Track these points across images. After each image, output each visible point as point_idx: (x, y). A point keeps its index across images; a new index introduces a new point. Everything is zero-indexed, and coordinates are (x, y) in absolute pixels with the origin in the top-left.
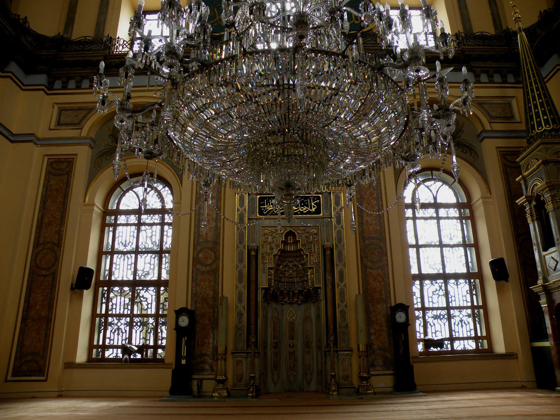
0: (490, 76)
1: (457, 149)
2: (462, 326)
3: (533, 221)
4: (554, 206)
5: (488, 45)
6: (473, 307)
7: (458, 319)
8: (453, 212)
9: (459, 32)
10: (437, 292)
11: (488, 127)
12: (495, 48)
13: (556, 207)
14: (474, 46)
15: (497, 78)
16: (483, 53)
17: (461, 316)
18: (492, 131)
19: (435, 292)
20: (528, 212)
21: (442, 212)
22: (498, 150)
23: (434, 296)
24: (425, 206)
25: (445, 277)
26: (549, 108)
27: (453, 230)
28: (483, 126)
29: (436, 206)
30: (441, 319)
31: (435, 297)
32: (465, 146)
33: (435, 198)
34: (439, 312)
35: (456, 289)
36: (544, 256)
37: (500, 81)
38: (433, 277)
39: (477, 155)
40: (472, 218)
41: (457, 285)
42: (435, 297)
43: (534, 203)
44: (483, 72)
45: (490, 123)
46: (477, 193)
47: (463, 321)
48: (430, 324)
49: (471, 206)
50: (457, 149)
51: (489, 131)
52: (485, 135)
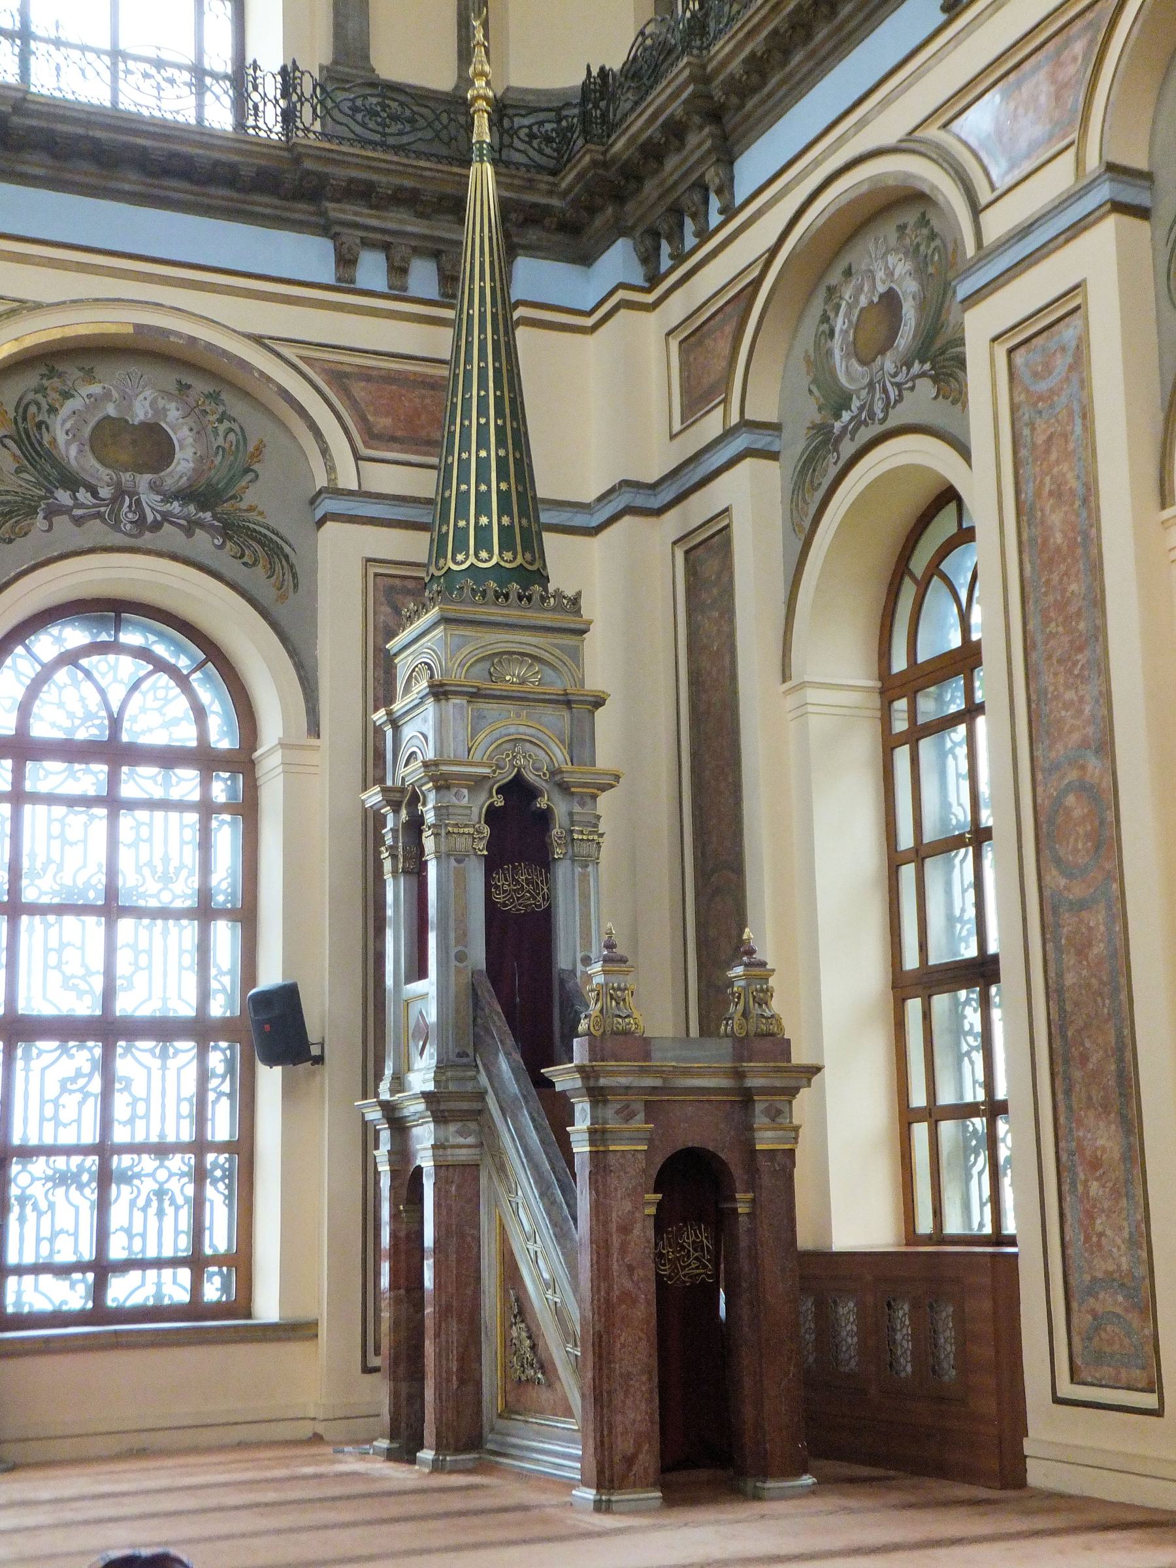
0: (398, 270)
1: (221, 547)
2: (160, 1213)
3: (395, 872)
4: (437, 845)
5: (398, 149)
6: (200, 1146)
7: (148, 1186)
8: (186, 783)
9: (295, 68)
10: (82, 1082)
11: (348, 479)
12: (422, 163)
13: (443, 849)
14: (341, 140)
15: (423, 277)
16: (375, 177)
17: (162, 1175)
18: (362, 494)
19: (73, 1080)
20: (389, 840)
21: (139, 782)
22: (373, 570)
23: (65, 1099)
24: (73, 752)
25: (108, 1030)
26: (503, 486)
27: (166, 847)
28: (331, 469)
29: (114, 751)
30: (81, 1187)
31: (70, 1101)
32: (254, 535)
33: (115, 723)
34: (76, 1160)
35: (156, 1075)
36: (407, 1003)
37: (433, 292)
38: (67, 1030)
39: (295, 576)
40: (247, 810)
41: (164, 1056)
42: (70, 1101)
43: (404, 815)
44: (366, 244)
45: (358, 457)
46: (273, 725)
47: (165, 1192)
48: (35, 1207)
49: (252, 763)
50: (221, 547)
51: (351, 493)
52: (329, 505)
